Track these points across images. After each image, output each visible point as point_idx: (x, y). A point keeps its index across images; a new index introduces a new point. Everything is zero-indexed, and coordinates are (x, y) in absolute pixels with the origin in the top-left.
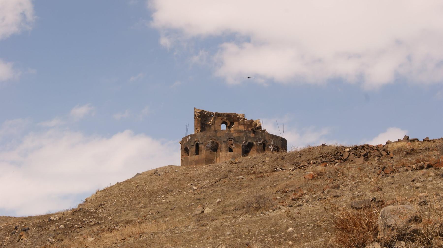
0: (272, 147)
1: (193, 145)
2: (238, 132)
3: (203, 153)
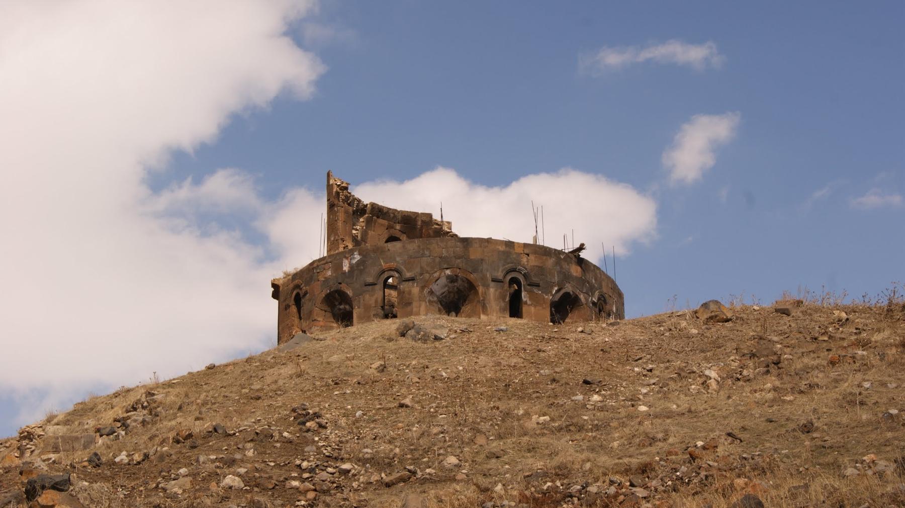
1: (374, 284)
2: (535, 253)
3: (415, 310)
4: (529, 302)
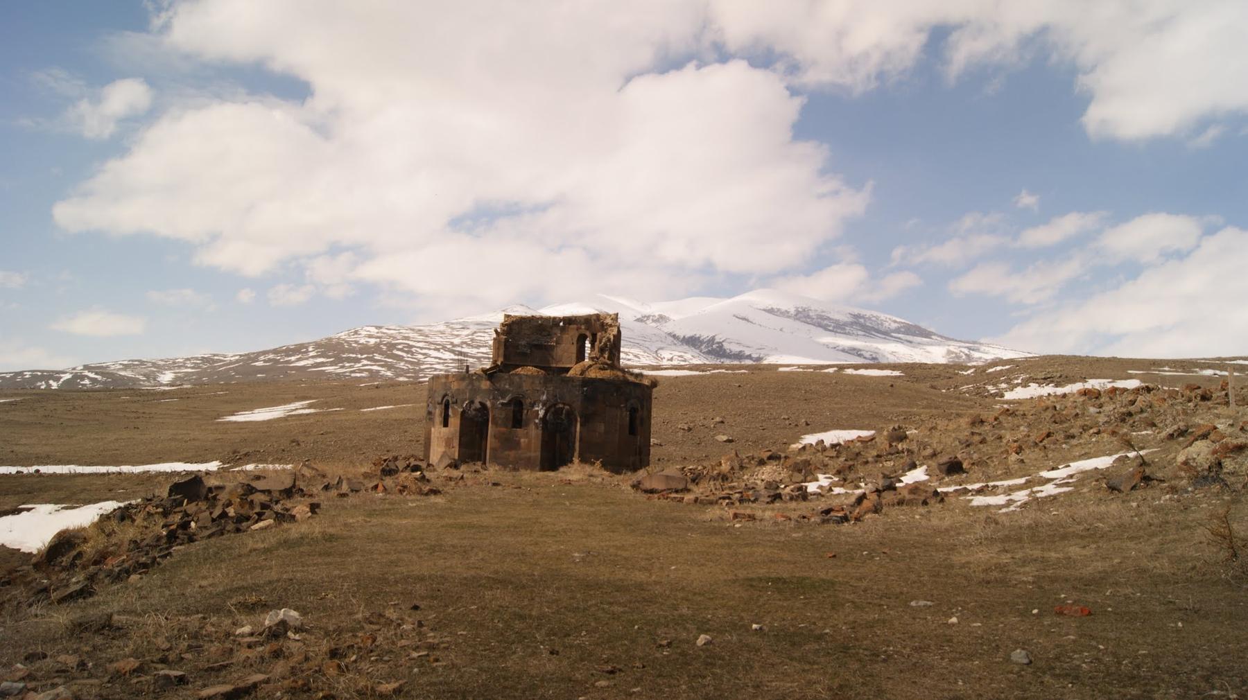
0: (541, 407)
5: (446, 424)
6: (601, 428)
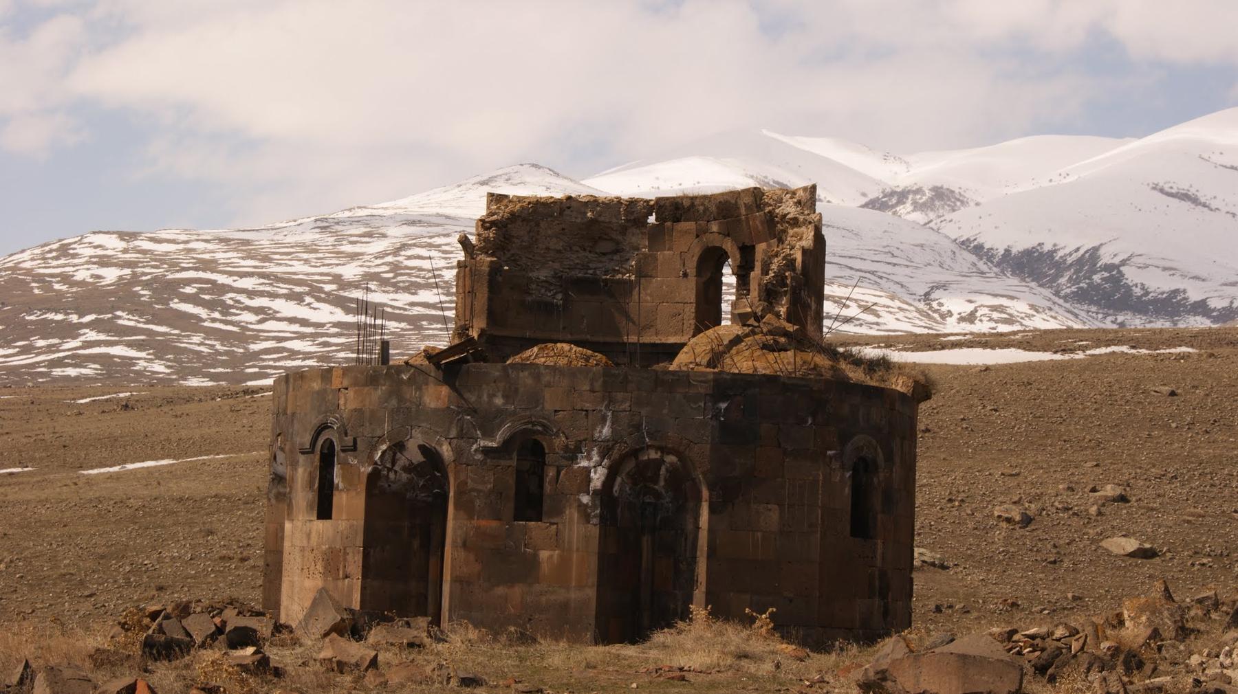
0: (596, 458)
4: (341, 486)
5: (324, 511)
6: (771, 517)
